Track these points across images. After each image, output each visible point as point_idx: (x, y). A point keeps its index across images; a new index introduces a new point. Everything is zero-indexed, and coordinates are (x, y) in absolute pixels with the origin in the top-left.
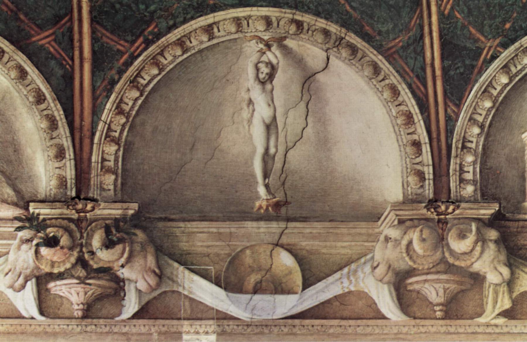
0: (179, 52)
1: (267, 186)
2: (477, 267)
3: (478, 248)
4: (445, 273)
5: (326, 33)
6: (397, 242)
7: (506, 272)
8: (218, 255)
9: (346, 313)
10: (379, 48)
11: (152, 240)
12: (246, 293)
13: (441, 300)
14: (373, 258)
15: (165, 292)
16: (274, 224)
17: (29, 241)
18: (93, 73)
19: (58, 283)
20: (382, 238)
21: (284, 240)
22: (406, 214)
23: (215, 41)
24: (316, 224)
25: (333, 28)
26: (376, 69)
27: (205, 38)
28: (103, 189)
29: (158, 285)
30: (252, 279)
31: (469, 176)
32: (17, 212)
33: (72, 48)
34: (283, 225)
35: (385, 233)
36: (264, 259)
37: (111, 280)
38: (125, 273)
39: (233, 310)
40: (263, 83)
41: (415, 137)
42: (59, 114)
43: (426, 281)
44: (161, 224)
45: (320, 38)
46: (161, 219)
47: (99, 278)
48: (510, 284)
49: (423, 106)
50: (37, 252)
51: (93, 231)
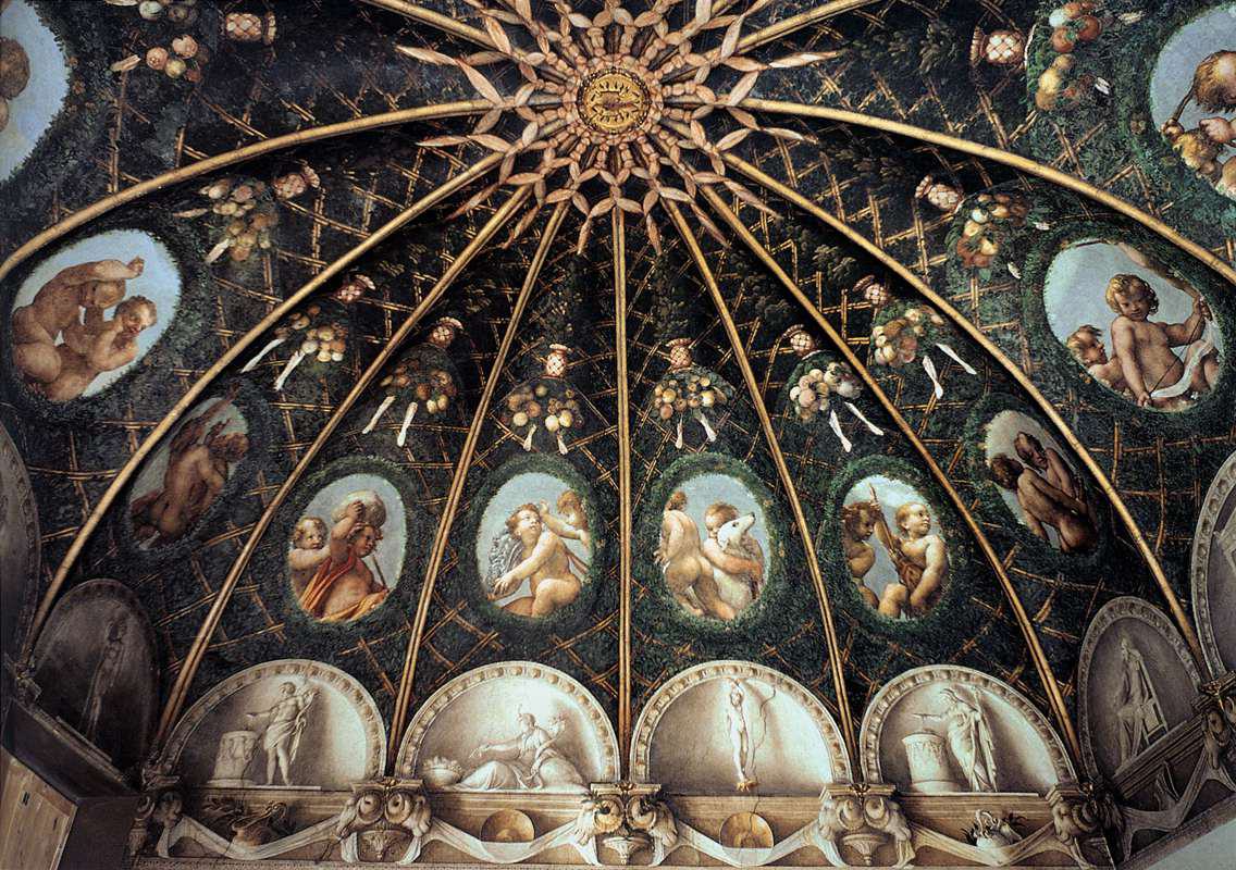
0: (682, 687)
1: (744, 773)
2: (888, 828)
3: (887, 815)
4: (868, 833)
5: (772, 675)
6: (833, 811)
7: (908, 832)
8: (715, 820)
9: (806, 862)
10: (805, 685)
11: (671, 810)
12: (737, 847)
13: (868, 852)
14: (818, 823)
15: (681, 847)
16: (751, 798)
17: (591, 810)
18: (631, 700)
19: (610, 839)
20: (823, 809)
21: (758, 810)
22: (836, 792)
23: (704, 681)
24: (780, 799)
25: (776, 673)
26: (806, 698)
27: (698, 678)
28: (637, 774)
29: (676, 843)
30: (739, 838)
31: (873, 767)
32: (584, 790)
33: (618, 683)
34: (757, 799)
35: (825, 804)
36: (746, 823)
37: (644, 838)
38: (654, 833)
39: (729, 860)
40: (736, 706)
41: (836, 741)
42: (609, 726)
43: (856, 839)
44: (676, 799)
45: (768, 678)
46: (676, 795)
47: (637, 836)
48: (912, 840)
49: (838, 720)
50: (596, 818)
51: (632, 803)
